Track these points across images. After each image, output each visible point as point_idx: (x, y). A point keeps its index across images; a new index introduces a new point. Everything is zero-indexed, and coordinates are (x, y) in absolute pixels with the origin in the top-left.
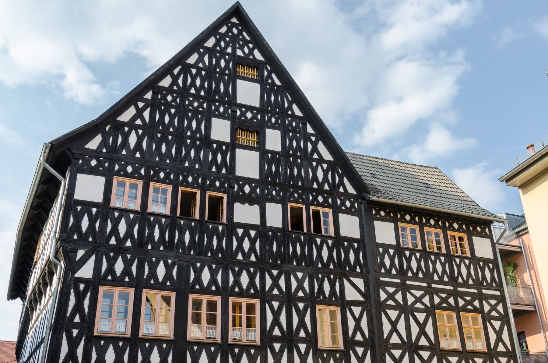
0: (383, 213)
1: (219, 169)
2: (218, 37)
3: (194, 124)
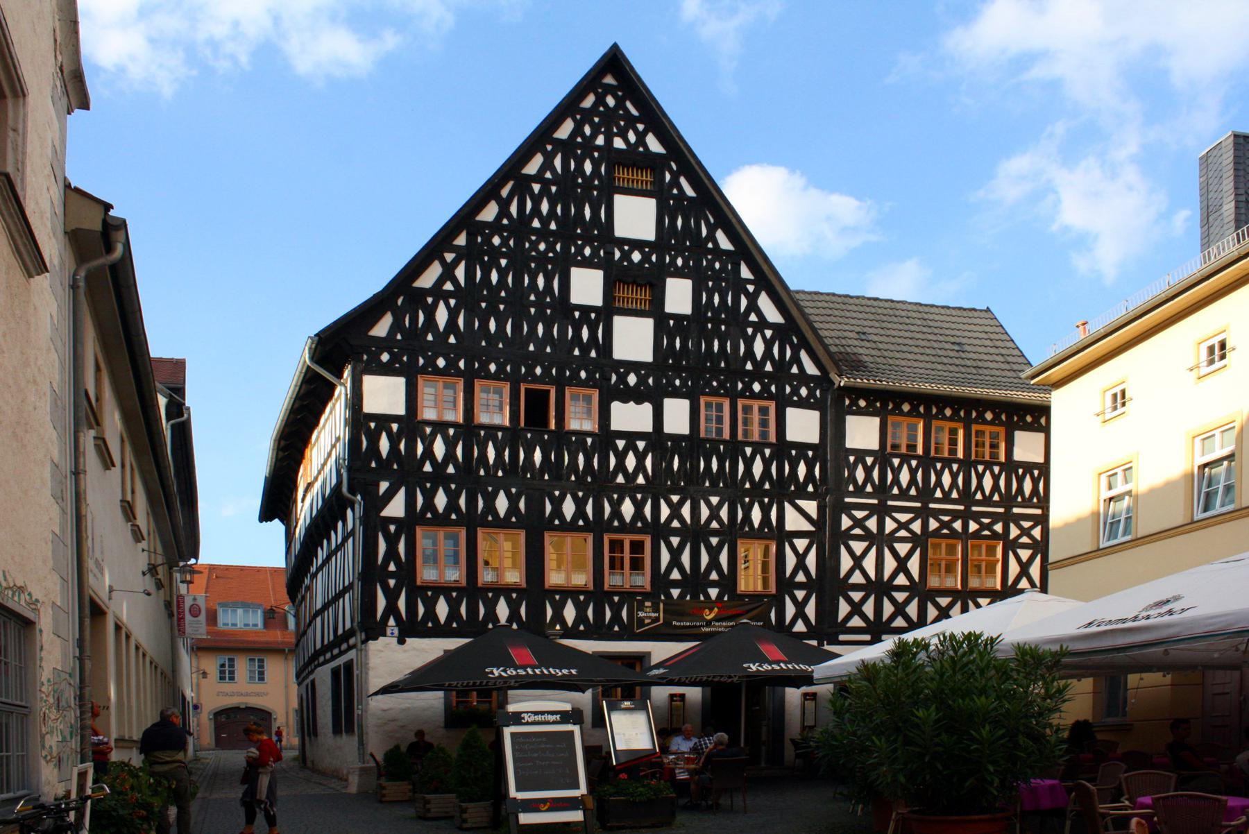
0: (862, 403)
1: (585, 349)
2: (578, 117)
3: (541, 281)
